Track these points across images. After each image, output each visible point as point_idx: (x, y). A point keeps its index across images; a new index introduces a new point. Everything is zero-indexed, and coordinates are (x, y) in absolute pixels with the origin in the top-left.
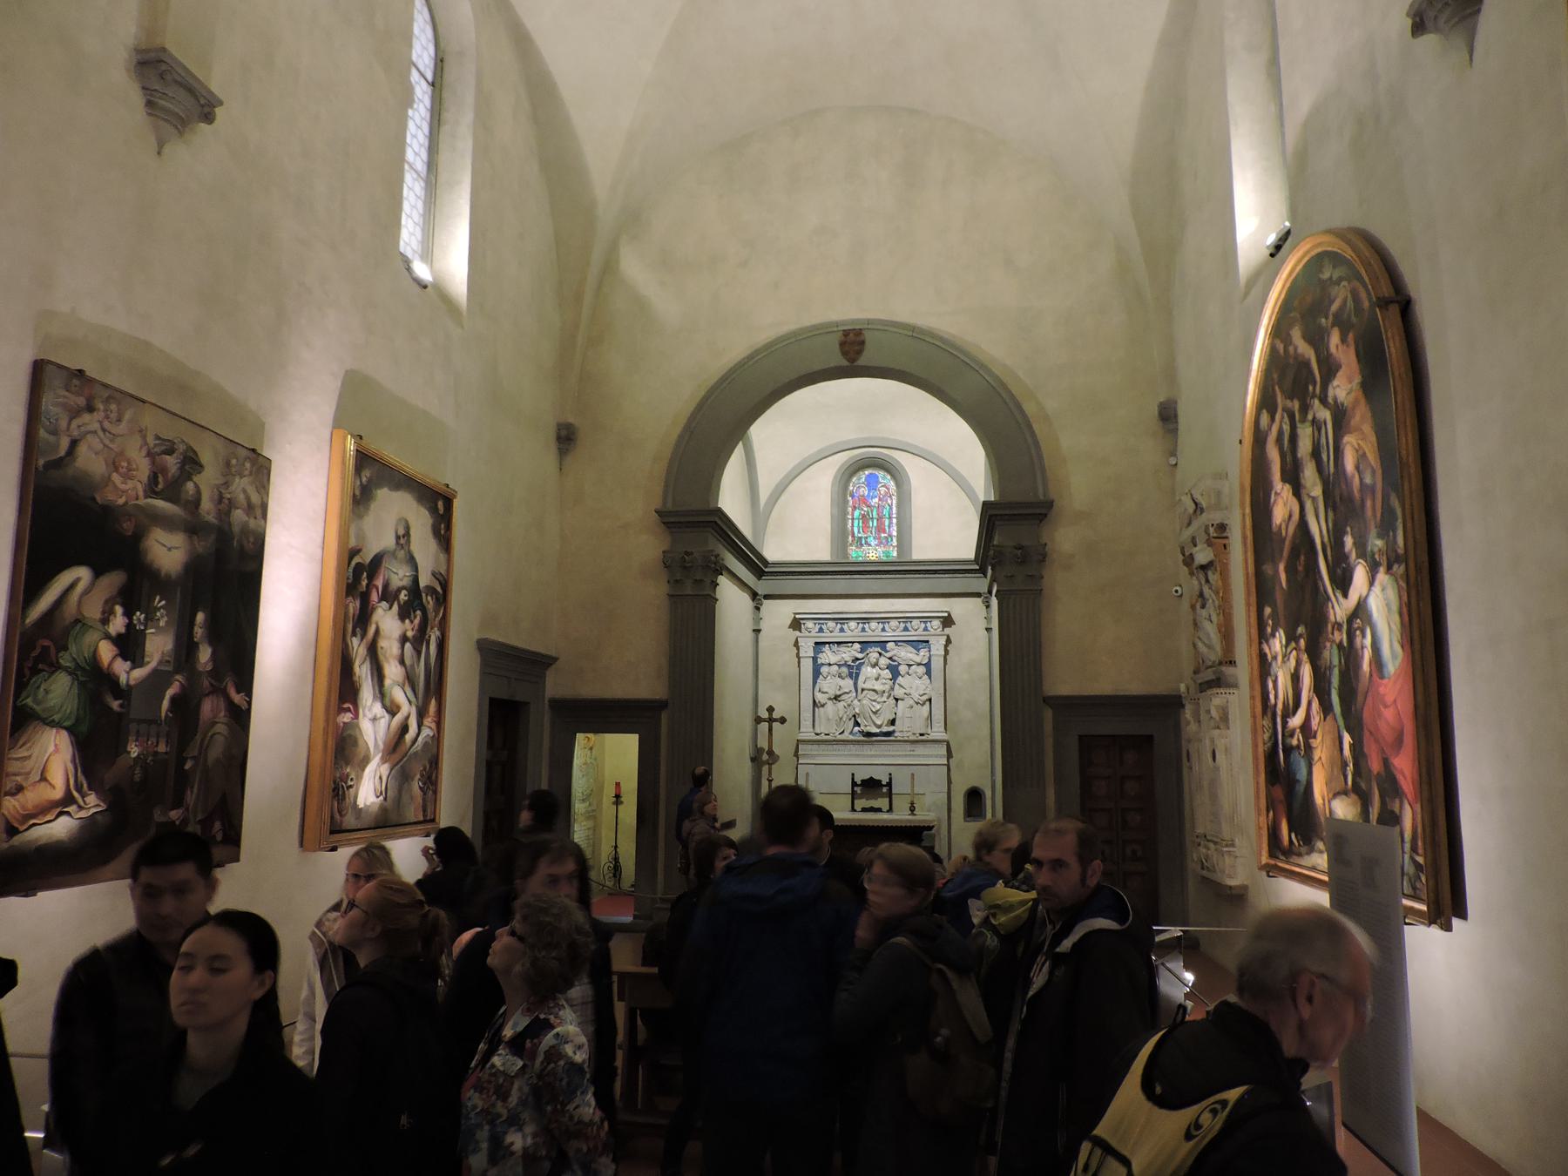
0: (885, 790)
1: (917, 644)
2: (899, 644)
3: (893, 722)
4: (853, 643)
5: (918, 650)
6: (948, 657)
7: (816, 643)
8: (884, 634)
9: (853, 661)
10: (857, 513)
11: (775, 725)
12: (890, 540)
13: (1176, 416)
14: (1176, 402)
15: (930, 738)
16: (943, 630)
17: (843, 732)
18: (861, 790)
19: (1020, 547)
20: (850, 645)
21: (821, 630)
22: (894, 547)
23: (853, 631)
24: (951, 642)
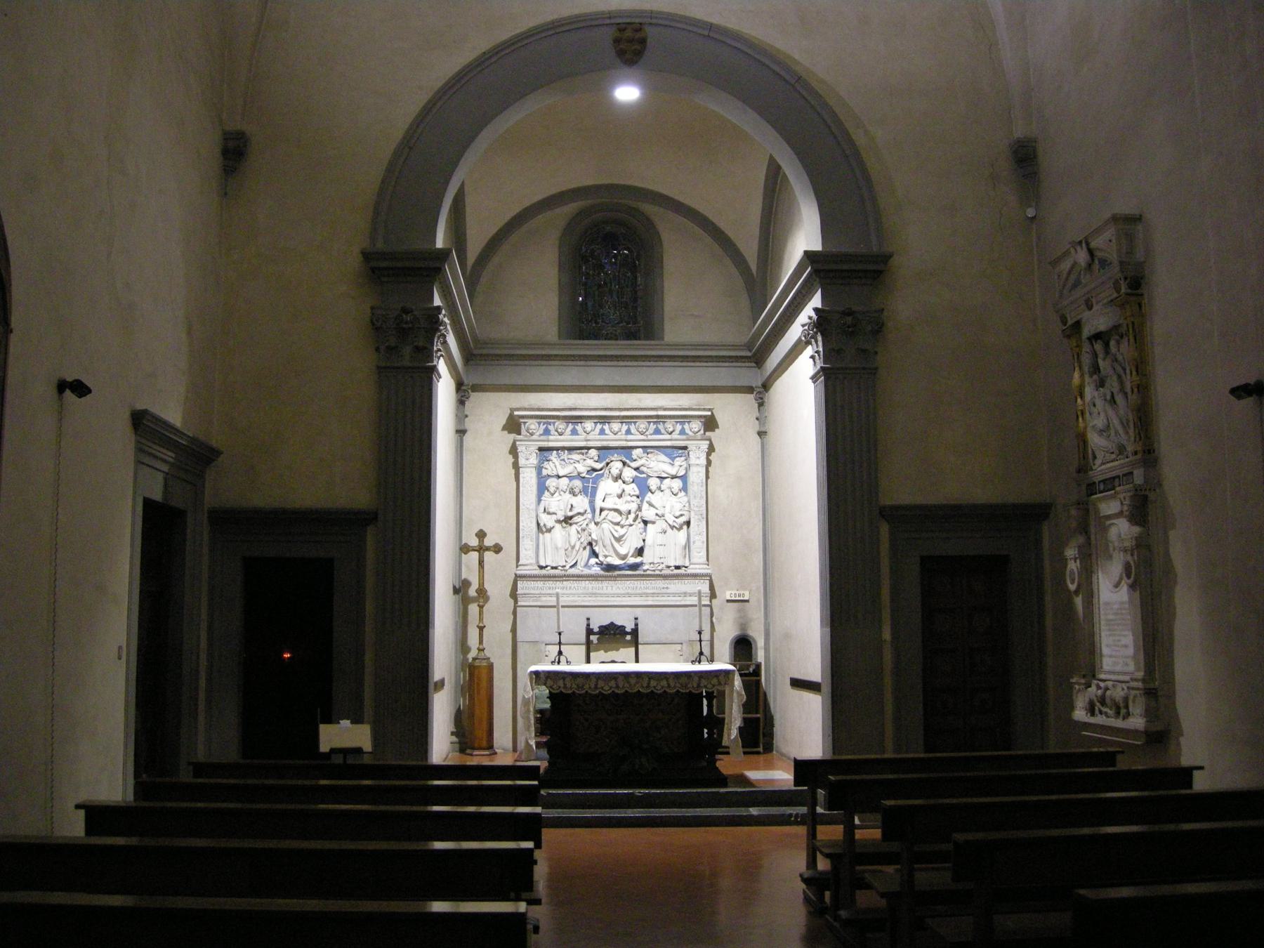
0: (628, 637)
3: (640, 551)
4: (589, 448)
6: (710, 469)
7: (541, 449)
8: (630, 437)
11: (488, 556)
13: (1035, 157)
15: (689, 571)
18: (598, 639)
19: (849, 313)
20: (584, 451)
21: (547, 432)
24: (714, 451)
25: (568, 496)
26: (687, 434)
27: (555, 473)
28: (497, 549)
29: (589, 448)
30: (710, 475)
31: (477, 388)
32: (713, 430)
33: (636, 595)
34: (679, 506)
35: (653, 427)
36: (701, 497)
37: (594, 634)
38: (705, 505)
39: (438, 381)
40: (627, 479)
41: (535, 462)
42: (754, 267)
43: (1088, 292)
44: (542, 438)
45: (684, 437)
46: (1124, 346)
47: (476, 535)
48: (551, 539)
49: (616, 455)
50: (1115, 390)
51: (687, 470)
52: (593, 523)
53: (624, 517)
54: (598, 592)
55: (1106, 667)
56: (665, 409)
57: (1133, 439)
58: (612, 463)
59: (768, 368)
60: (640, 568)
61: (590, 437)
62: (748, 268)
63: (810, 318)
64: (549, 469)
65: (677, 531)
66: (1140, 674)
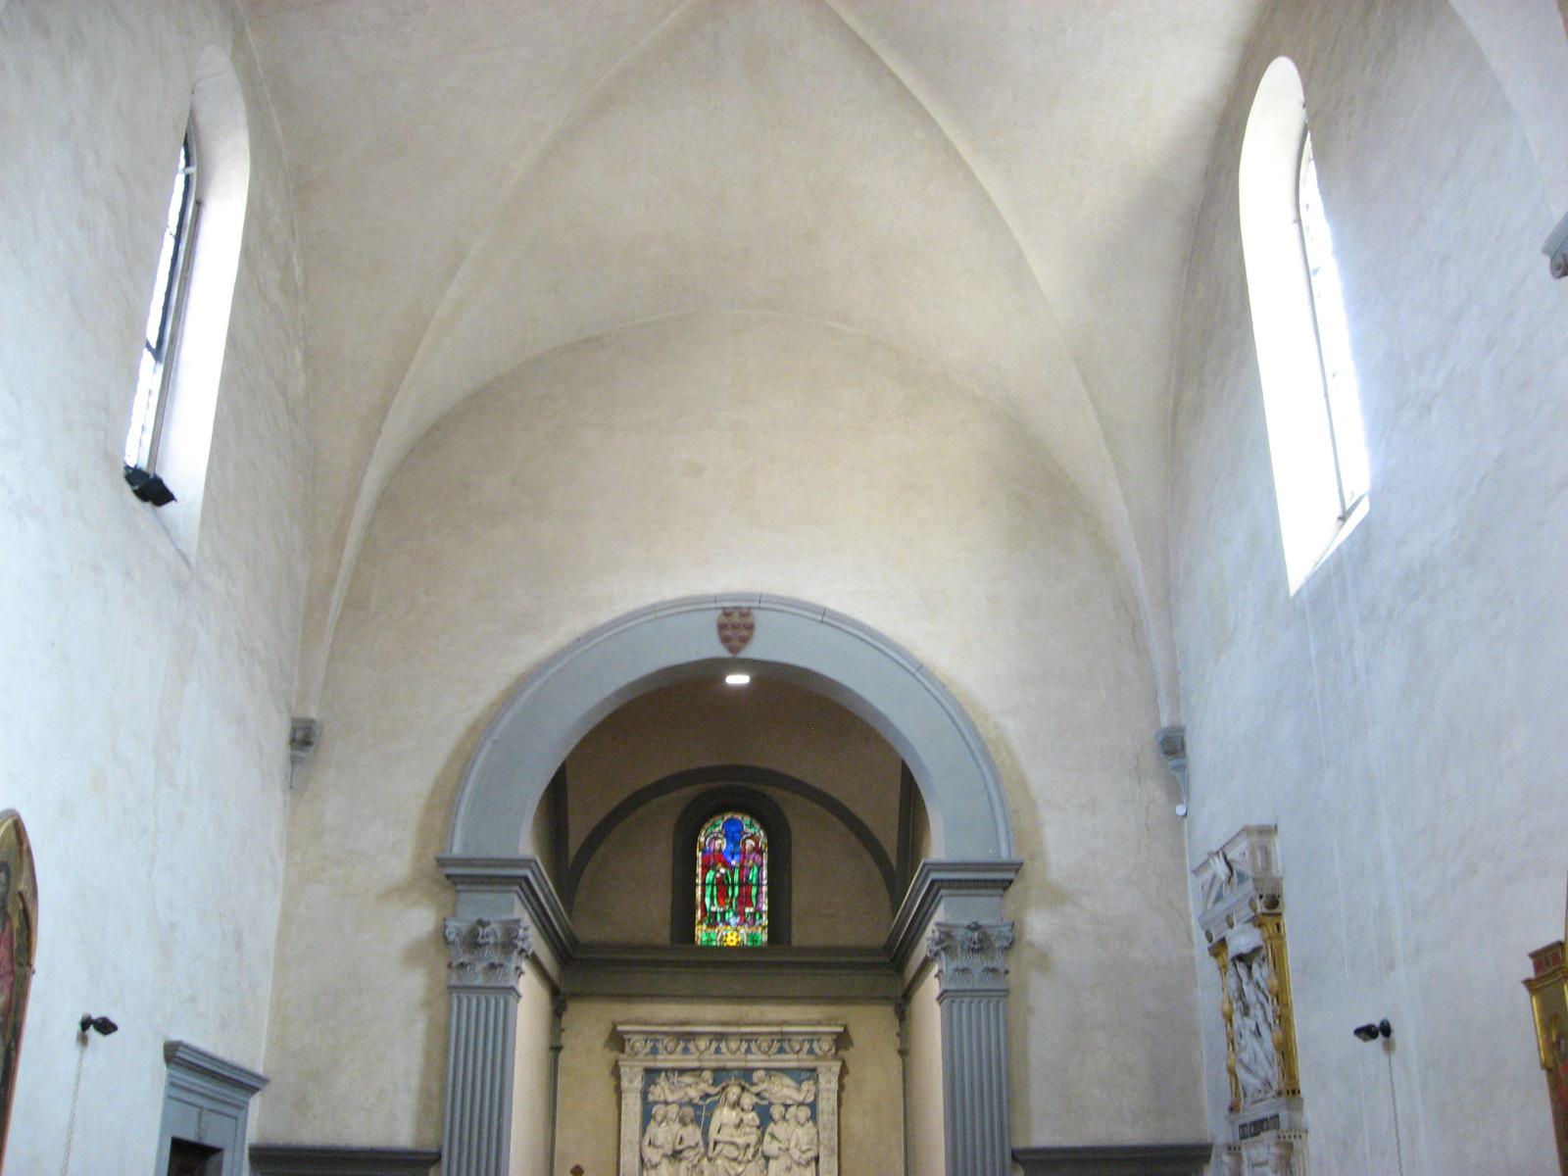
1: (799, 1075)
2: (772, 1073)
4: (701, 1070)
5: (800, 1083)
6: (844, 1095)
8: (750, 1057)
9: (701, 1098)
10: (710, 876)
12: (757, 916)
13: (1183, 748)
14: (1182, 730)
16: (836, 1053)
19: (976, 927)
20: (698, 1073)
22: (764, 928)
23: (703, 1054)
25: (677, 1126)
27: (662, 1098)
30: (844, 1101)
31: (578, 996)
32: (847, 1049)
36: (832, 1129)
39: (518, 1001)
40: (745, 1107)
41: (640, 1086)
42: (894, 860)
44: (648, 1057)
45: (812, 1057)
46: (1265, 970)
50: (1260, 1020)
51: (816, 1097)
52: (706, 1160)
53: (742, 1152)
58: (729, 1088)
59: (906, 976)
61: (706, 1056)
62: (888, 862)
63: (933, 932)
64: (658, 1092)
65: (803, 1169)
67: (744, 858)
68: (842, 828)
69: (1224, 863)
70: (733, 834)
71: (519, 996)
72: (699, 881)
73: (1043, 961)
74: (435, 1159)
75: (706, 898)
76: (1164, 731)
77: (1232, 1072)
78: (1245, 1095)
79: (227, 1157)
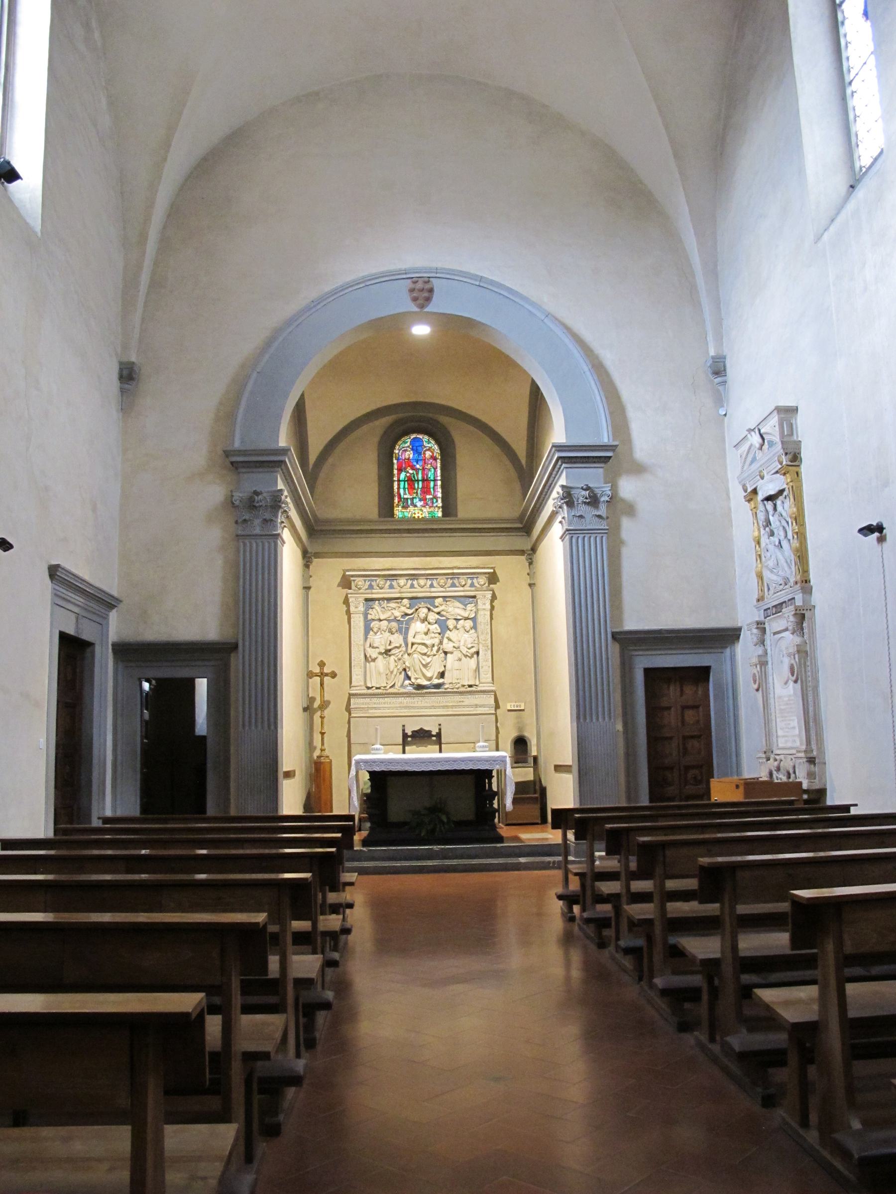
3: (442, 675)
4: (402, 599)
7: (367, 600)
8: (433, 589)
12: (435, 500)
13: (725, 370)
14: (725, 358)
15: (479, 689)
16: (489, 586)
17: (393, 686)
19: (588, 488)
21: (371, 587)
22: (439, 507)
23: (403, 587)
24: (496, 599)
25: (387, 634)
26: (475, 587)
27: (377, 617)
28: (333, 675)
29: (402, 599)
30: (494, 616)
31: (318, 555)
32: (495, 583)
33: (439, 707)
34: (469, 640)
35: (450, 581)
36: (487, 633)
37: (409, 736)
38: (489, 640)
39: (283, 546)
40: (431, 621)
41: (362, 609)
43: (761, 466)
45: (473, 589)
47: (318, 664)
48: (375, 667)
49: (423, 603)
50: (782, 538)
52: (406, 654)
53: (430, 649)
54: (411, 705)
55: (780, 745)
56: (459, 568)
57: (794, 573)
60: (442, 687)
62: (519, 461)
63: (558, 493)
64: (373, 614)
65: (469, 659)
66: (804, 747)
67: (425, 463)
68: (487, 440)
69: (759, 436)
70: (416, 448)
71: (284, 542)
72: (395, 479)
73: (630, 510)
74: (234, 647)
75: (401, 489)
76: (713, 358)
77: (760, 577)
78: (769, 589)
79: (98, 649)
